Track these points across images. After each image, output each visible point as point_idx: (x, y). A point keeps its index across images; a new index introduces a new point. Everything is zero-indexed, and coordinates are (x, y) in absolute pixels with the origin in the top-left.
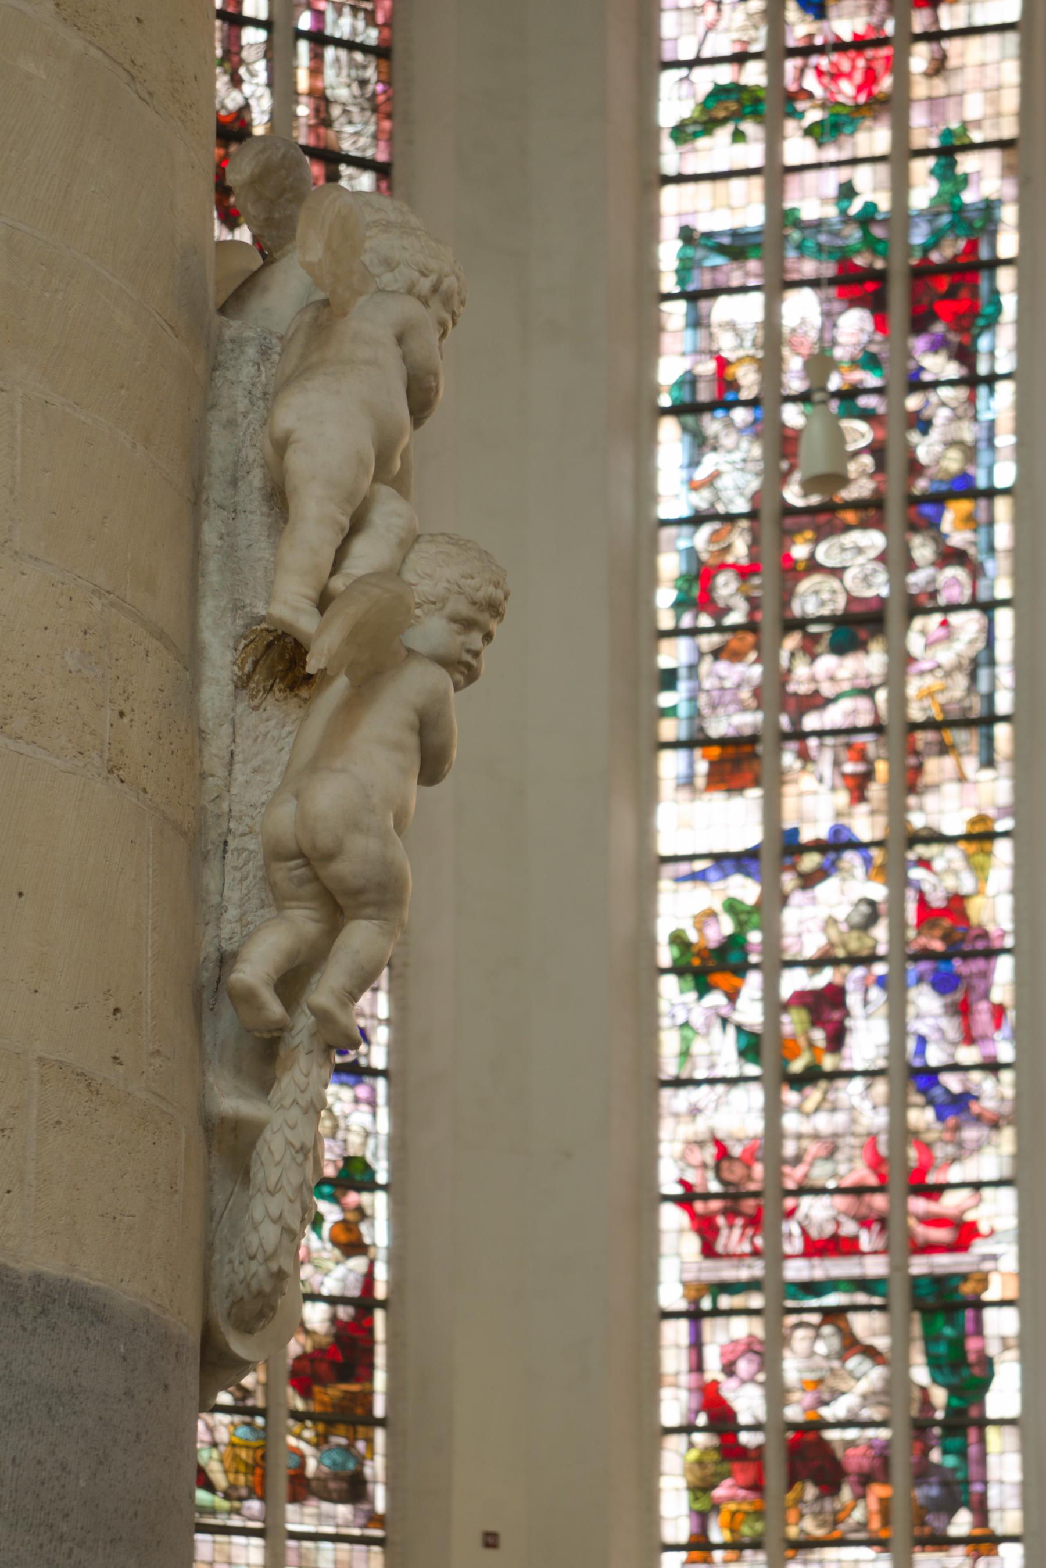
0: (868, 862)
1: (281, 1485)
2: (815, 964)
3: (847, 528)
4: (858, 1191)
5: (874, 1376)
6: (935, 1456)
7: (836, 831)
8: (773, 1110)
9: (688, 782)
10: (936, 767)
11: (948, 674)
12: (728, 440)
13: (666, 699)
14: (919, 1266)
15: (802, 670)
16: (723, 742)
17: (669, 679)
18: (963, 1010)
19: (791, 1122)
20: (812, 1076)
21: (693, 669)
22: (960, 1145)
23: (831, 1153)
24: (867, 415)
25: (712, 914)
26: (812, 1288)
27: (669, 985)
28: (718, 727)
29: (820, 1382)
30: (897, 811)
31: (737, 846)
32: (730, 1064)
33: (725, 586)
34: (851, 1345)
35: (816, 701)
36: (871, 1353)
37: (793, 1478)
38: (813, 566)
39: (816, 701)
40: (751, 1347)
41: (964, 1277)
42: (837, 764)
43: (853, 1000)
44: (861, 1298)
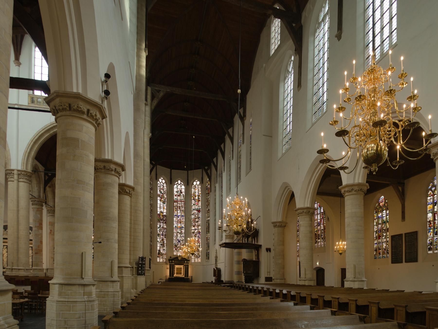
10: (199, 227)
17: (192, 223)
20: (196, 237)
30: (198, 228)
33: (194, 220)
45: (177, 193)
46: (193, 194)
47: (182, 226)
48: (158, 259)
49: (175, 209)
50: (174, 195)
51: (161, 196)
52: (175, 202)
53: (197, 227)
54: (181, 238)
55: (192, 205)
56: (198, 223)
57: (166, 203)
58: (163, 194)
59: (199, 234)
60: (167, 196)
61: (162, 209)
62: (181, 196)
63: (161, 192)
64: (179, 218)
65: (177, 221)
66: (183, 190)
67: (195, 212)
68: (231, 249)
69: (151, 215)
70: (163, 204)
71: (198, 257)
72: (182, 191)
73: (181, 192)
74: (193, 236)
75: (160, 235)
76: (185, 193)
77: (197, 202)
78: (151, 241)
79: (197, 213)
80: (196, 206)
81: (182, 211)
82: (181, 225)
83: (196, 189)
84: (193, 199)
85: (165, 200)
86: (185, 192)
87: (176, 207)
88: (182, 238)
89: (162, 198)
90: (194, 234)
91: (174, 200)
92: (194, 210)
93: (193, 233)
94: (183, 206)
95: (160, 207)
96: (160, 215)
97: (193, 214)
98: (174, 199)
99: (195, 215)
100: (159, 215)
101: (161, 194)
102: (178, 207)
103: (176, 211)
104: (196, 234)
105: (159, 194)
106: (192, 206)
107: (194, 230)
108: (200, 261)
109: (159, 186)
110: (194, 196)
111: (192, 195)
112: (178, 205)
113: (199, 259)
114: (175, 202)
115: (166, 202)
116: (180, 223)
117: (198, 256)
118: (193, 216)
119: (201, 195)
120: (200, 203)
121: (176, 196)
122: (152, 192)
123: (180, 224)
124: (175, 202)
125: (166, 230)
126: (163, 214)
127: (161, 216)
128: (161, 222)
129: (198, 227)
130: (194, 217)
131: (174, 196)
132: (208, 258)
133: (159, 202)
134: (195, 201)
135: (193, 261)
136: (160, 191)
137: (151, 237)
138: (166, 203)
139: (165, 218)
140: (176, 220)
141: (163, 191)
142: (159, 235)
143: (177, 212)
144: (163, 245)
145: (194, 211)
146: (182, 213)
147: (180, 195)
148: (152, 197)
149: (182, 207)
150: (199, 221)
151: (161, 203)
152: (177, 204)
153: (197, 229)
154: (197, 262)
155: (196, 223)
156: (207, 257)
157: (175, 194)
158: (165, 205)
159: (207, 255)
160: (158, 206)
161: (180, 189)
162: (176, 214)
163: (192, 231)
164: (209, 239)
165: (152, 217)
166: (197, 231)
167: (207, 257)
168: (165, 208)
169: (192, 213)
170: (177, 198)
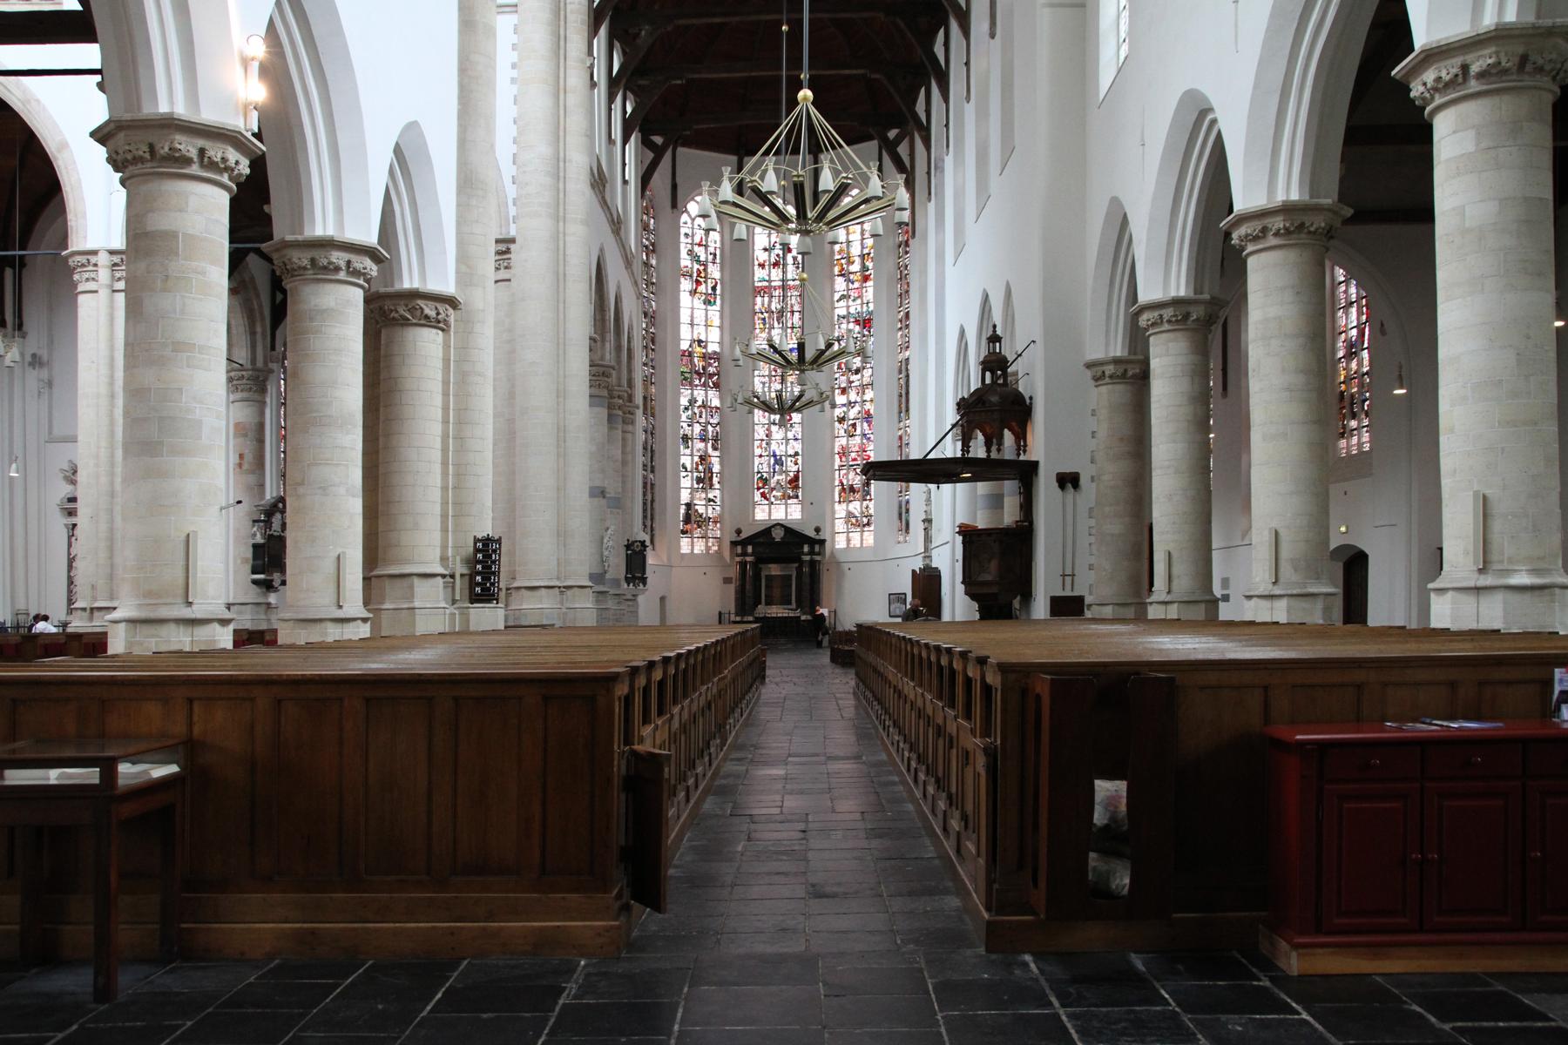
1: (786, 497)
8: (848, 440)
10: (867, 391)
17: (836, 379)
18: (869, 426)
19: (850, 442)
26: (852, 466)
27: (836, 423)
30: (862, 397)
32: (843, 434)
34: (857, 474)
35: (853, 382)
37: (850, 492)
39: (853, 382)
40: (845, 474)
45: (770, 256)
46: (839, 253)
48: (682, 544)
49: (758, 324)
50: (754, 265)
51: (695, 275)
52: (759, 292)
55: (837, 296)
56: (863, 376)
57: (718, 301)
58: (705, 266)
59: (865, 424)
60: (722, 270)
61: (702, 329)
62: (785, 265)
63: (696, 258)
65: (770, 372)
68: (953, 484)
69: (652, 360)
70: (704, 307)
71: (864, 526)
74: (842, 432)
75: (692, 439)
77: (856, 285)
78: (652, 467)
79: (859, 333)
80: (851, 303)
81: (792, 328)
83: (851, 231)
85: (714, 288)
87: (762, 313)
89: (698, 283)
90: (845, 427)
91: (755, 288)
92: (845, 321)
93: (841, 420)
94: (796, 308)
95: (692, 320)
96: (690, 354)
98: (756, 279)
100: (687, 354)
101: (696, 266)
102: (773, 312)
103: (762, 330)
104: (854, 425)
106: (836, 305)
107: (845, 409)
108: (869, 538)
109: (686, 235)
110: (843, 261)
111: (837, 257)
113: (865, 534)
114: (758, 291)
115: (718, 297)
119: (872, 251)
120: (871, 290)
121: (762, 266)
122: (654, 262)
124: (758, 291)
125: (721, 416)
126: (705, 347)
127: (696, 360)
128: (697, 382)
129: (864, 393)
131: (756, 267)
132: (904, 531)
133: (685, 299)
134: (849, 281)
135: (840, 543)
136: (690, 252)
137: (652, 451)
138: (718, 301)
139: (716, 364)
141: (706, 253)
142: (686, 438)
144: (705, 481)
145: (844, 326)
148: (653, 284)
149: (792, 312)
150: (864, 368)
151: (698, 303)
152: (770, 302)
154: (859, 546)
155: (854, 378)
156: (901, 522)
157: (761, 261)
158: (714, 313)
159: (900, 515)
160: (684, 316)
163: (838, 412)
164: (908, 444)
165: (653, 367)
166: (857, 408)
167: (901, 522)
168: (716, 321)
170: (769, 275)
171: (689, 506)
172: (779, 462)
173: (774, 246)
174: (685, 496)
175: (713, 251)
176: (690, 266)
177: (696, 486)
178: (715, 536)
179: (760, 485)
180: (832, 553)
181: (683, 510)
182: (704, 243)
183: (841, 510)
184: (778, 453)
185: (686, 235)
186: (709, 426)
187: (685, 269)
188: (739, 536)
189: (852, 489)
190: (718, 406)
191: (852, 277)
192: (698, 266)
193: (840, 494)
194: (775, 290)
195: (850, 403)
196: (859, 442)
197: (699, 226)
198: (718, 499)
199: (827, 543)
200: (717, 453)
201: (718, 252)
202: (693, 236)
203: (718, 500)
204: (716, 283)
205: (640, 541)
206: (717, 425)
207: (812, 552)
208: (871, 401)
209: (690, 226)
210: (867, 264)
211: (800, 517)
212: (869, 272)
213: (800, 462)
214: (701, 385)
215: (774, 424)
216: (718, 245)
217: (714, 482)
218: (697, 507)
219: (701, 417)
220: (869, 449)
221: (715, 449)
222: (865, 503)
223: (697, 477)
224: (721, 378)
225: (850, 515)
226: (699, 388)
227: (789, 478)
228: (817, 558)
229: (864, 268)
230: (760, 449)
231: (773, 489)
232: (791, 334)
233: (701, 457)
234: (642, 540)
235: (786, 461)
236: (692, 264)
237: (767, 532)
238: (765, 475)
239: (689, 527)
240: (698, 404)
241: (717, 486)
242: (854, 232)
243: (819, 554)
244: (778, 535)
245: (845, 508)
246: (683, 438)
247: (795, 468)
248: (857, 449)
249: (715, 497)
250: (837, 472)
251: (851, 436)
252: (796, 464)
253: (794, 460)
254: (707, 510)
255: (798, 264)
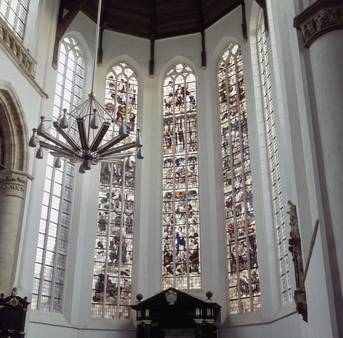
0: (242, 190)
2: (238, 202)
3: (238, 154)
4: (244, 227)
5: (246, 249)
6: (252, 257)
7: (239, 187)
8: (235, 219)
9: (226, 185)
10: (247, 177)
11: (248, 167)
12: (228, 148)
13: (224, 176)
14: (250, 235)
15: (235, 170)
16: (229, 180)
17: (224, 174)
21: (226, 173)
22: (252, 220)
23: (241, 224)
24: (239, 142)
25: (229, 199)
26: (241, 239)
28: (229, 178)
29: (241, 250)
31: (231, 191)
34: (244, 246)
36: (246, 246)
38: (236, 159)
41: (253, 235)
42: (239, 179)
43: (242, 205)
44: (245, 240)
46: (222, 87)
47: (189, 190)
51: (117, 110)
52: (167, 122)
53: (241, 182)
54: (189, 227)
64: (181, 168)
66: (192, 87)
67: (231, 136)
71: (253, 291)
72: (189, 90)
73: (185, 91)
76: (197, 95)
77: (234, 105)
80: (232, 117)
82: (187, 186)
84: (223, 99)
85: (132, 120)
86: (196, 91)
87: (169, 136)
88: (193, 230)
97: (225, 146)
99: (233, 144)
101: (118, 105)
104: (240, 207)
105: (111, 104)
110: (224, 92)
111: (220, 91)
112: (177, 130)
113: (256, 299)
115: (136, 126)
116: (184, 181)
117: (253, 285)
118: (226, 149)
121: (168, 105)
123: (184, 185)
129: (246, 180)
130: (229, 152)
136: (113, 96)
140: (170, 174)
143: (175, 151)
145: (228, 135)
146: (190, 151)
147: (182, 101)
149: (191, 133)
150: (244, 160)
153: (239, 189)
157: (167, 102)
161: (183, 85)
162: (169, 158)
169: (223, 142)
170: (173, 111)
171: (101, 277)
172: (182, 242)
173: (177, 92)
174: (98, 269)
175: (132, 96)
176: (113, 104)
177: (110, 261)
178: (126, 304)
179: (167, 261)
180: (228, 318)
181: (95, 281)
182: (125, 91)
183: (234, 280)
184: (181, 235)
185: (111, 85)
186: (125, 215)
187: (109, 106)
188: (139, 301)
189: (241, 260)
190: (133, 200)
191: (231, 99)
192: (119, 105)
193: (231, 266)
194: (178, 119)
195: (235, 189)
196: (244, 219)
197: (122, 80)
198: (131, 272)
199: (221, 309)
200: (130, 236)
201: (136, 97)
202: (116, 86)
203: (130, 273)
204: (134, 117)
205: (18, 298)
206: (131, 214)
207: (204, 316)
208: (251, 184)
209: (115, 80)
210: (242, 87)
211: (200, 288)
212: (243, 92)
213: (199, 241)
214: (118, 184)
215: (178, 212)
216: (136, 93)
217: (127, 259)
218: (110, 278)
219: (117, 207)
220: (252, 223)
221: (129, 232)
222: (253, 271)
223: (111, 253)
224: (136, 180)
225: (241, 282)
226: (116, 186)
227: (190, 255)
228: (211, 321)
229: (240, 90)
230: (166, 233)
231: (177, 265)
232: (190, 146)
233: (115, 238)
234: (23, 297)
235: (188, 241)
236: (115, 102)
237: (161, 296)
238: (170, 253)
239: (101, 294)
240: (115, 198)
241: (130, 262)
242: (231, 71)
243: (210, 317)
244: (172, 299)
245: (236, 277)
246: (100, 223)
247: (194, 247)
248: (243, 225)
249: (127, 270)
250: (229, 247)
251: (237, 216)
252: (196, 243)
253: (193, 240)
254: (119, 281)
255: (194, 101)
